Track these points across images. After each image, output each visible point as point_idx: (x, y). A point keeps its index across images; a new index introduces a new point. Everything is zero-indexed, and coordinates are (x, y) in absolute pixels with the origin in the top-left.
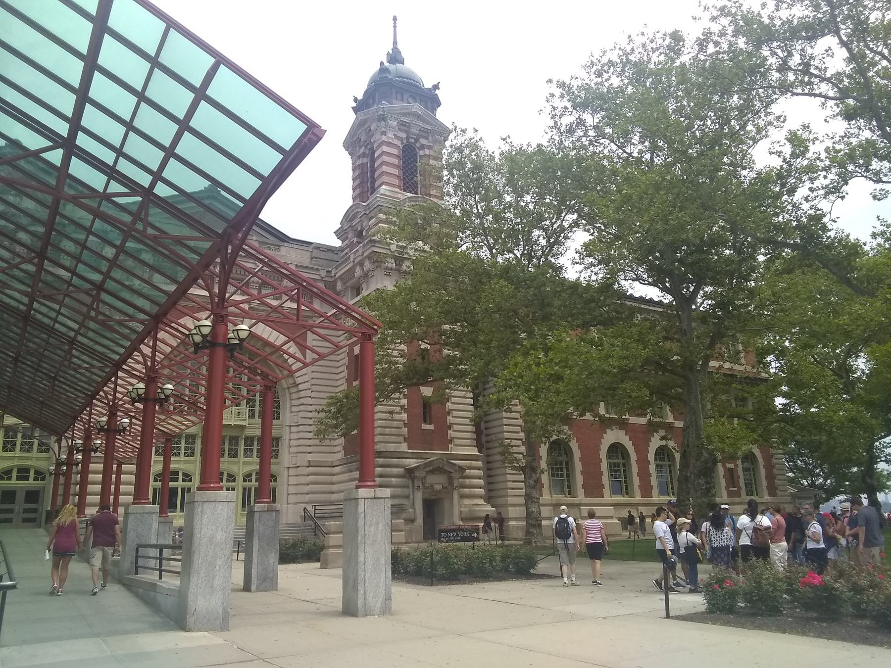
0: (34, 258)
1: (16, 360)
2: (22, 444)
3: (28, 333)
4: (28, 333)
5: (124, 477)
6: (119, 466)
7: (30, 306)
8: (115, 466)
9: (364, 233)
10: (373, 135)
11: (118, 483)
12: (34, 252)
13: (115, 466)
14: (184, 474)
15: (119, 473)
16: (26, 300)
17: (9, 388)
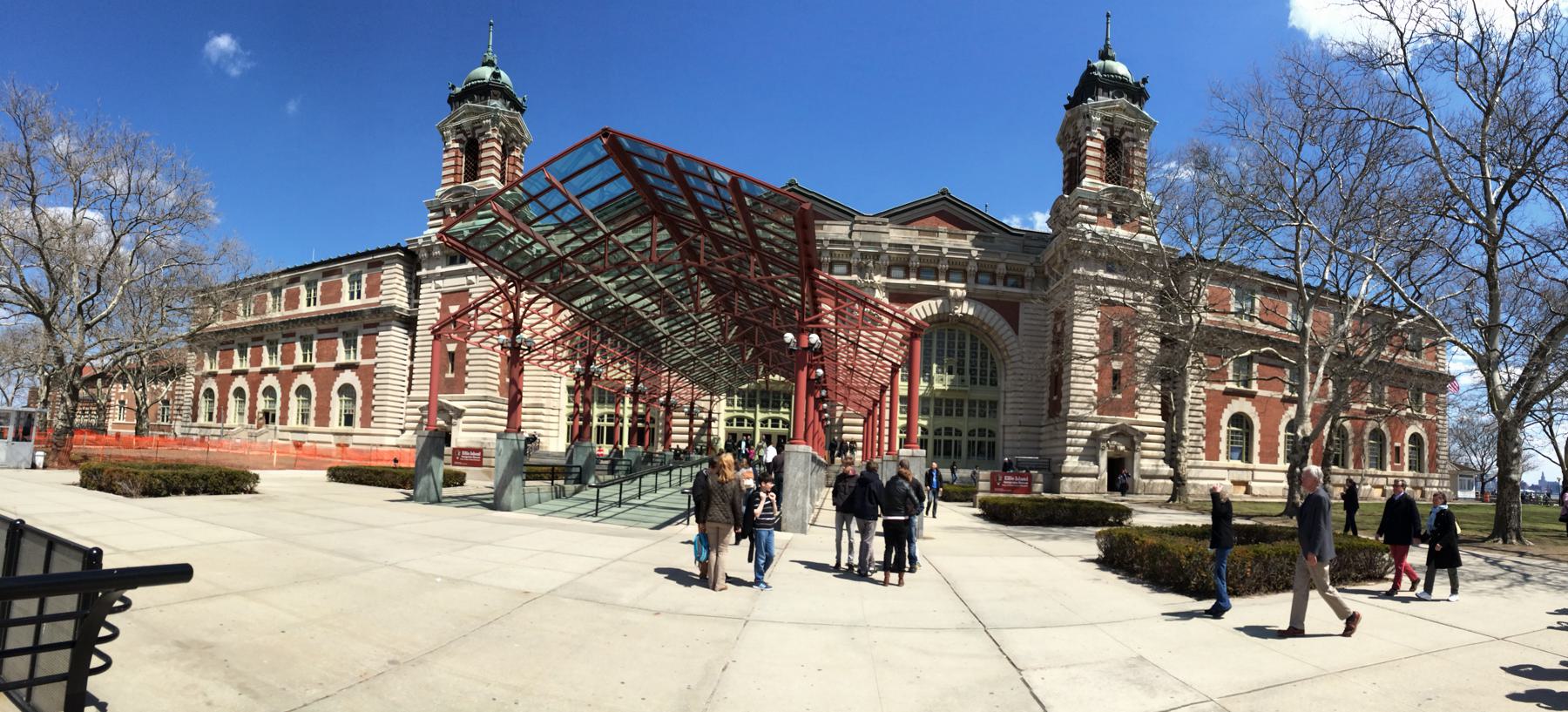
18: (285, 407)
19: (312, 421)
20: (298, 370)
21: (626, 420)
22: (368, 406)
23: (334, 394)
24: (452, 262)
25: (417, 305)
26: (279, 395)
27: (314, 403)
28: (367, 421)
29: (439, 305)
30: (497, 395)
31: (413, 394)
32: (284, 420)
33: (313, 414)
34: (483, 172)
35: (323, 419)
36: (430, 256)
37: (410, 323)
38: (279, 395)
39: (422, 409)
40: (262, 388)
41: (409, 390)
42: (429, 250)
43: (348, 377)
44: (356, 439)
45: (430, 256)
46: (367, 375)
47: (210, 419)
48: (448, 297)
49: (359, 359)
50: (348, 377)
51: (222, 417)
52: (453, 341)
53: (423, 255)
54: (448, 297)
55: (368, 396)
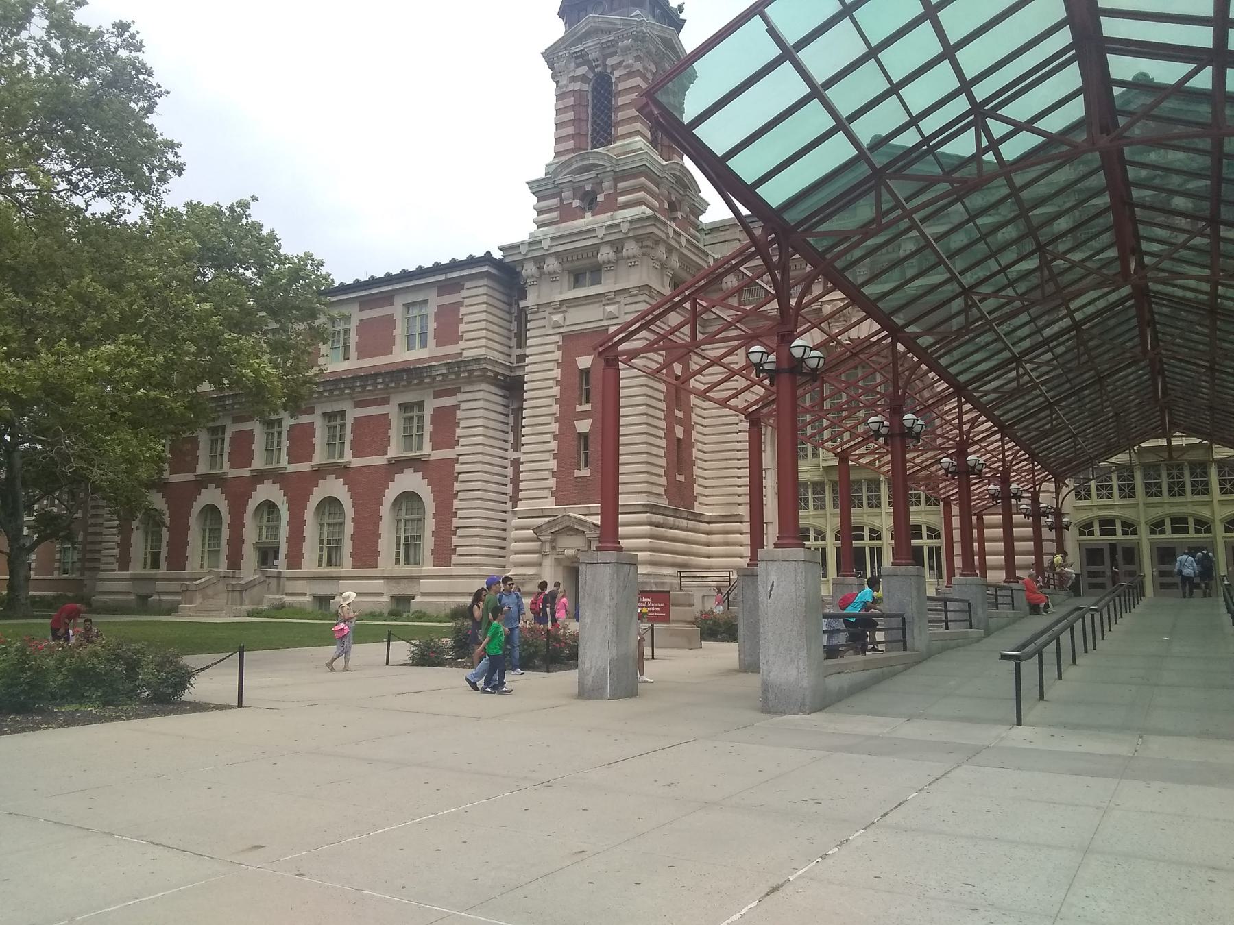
0: (1204, 228)
1: (1212, 369)
2: (1193, 485)
3: (1221, 330)
4: (1221, 330)
5: (988, 532)
6: (980, 518)
7: (1214, 295)
8: (974, 518)
9: (600, 198)
10: (614, 54)
11: (982, 540)
12: (1202, 219)
13: (974, 518)
14: (816, 531)
15: (981, 526)
16: (1206, 287)
17: (1211, 408)
18: (296, 538)
19: (347, 560)
20: (321, 472)
21: (830, 537)
22: (445, 531)
23: (385, 509)
24: (577, 279)
25: (522, 358)
26: (226, 518)
27: (349, 529)
28: (443, 554)
29: (558, 355)
30: (664, 502)
31: (521, 506)
32: (295, 560)
33: (348, 546)
34: (622, 130)
35: (366, 555)
36: (542, 274)
37: (512, 387)
38: (226, 518)
39: (537, 529)
40: (252, 504)
41: (515, 500)
42: (539, 261)
43: (410, 481)
44: (426, 585)
45: (542, 274)
46: (442, 477)
47: (155, 564)
48: (572, 341)
49: (427, 448)
50: (410, 481)
51: (178, 559)
52: (584, 415)
53: (529, 270)
54: (572, 341)
55: (445, 512)
